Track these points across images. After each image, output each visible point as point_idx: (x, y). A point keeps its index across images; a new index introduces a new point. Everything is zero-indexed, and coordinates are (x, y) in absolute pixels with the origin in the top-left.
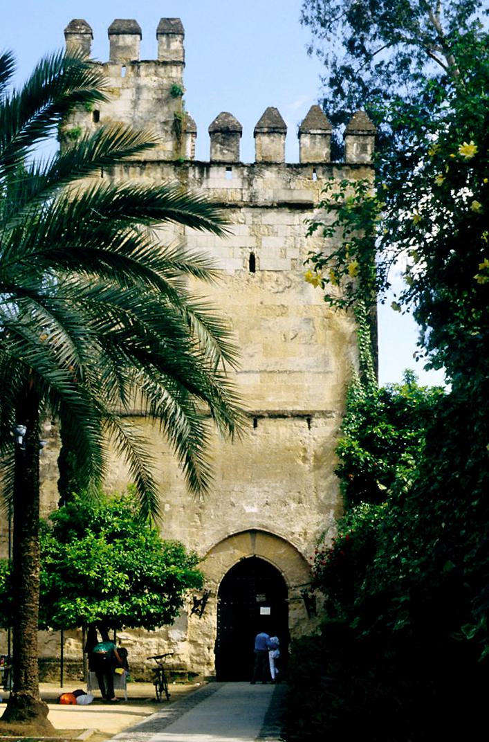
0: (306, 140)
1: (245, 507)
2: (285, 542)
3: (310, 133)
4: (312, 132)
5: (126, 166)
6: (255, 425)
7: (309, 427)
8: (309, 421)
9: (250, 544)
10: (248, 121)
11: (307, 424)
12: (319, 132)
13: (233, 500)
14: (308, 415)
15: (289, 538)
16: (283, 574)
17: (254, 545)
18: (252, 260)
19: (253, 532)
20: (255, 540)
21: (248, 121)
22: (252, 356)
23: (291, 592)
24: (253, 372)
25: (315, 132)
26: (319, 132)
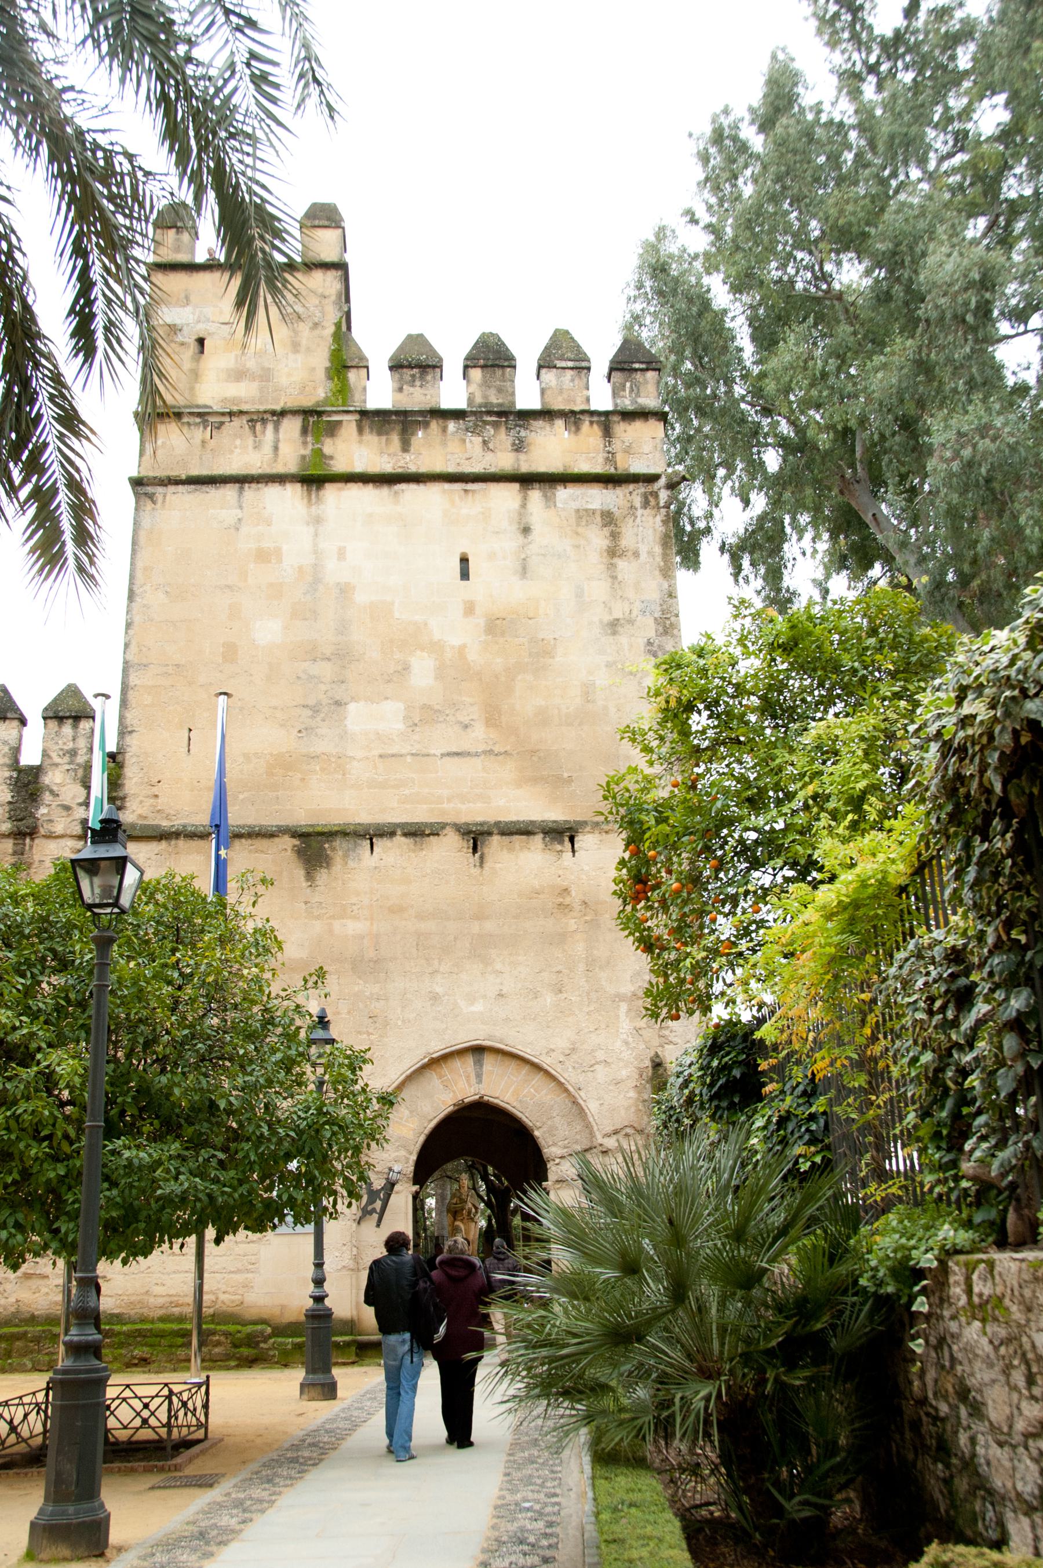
0: (549, 376)
1: (462, 1004)
2: (537, 1067)
3: (555, 367)
4: (560, 364)
5: (251, 421)
6: (475, 849)
7: (573, 851)
8: (572, 840)
9: (473, 1076)
10: (453, 355)
11: (568, 844)
12: (570, 364)
13: (439, 990)
14: (570, 829)
15: (546, 1061)
16: (536, 1133)
17: (479, 1077)
18: (464, 560)
19: (478, 1050)
20: (481, 1066)
21: (453, 355)
22: (466, 727)
23: (554, 1168)
24: (469, 754)
25: (563, 364)
26: (570, 364)
